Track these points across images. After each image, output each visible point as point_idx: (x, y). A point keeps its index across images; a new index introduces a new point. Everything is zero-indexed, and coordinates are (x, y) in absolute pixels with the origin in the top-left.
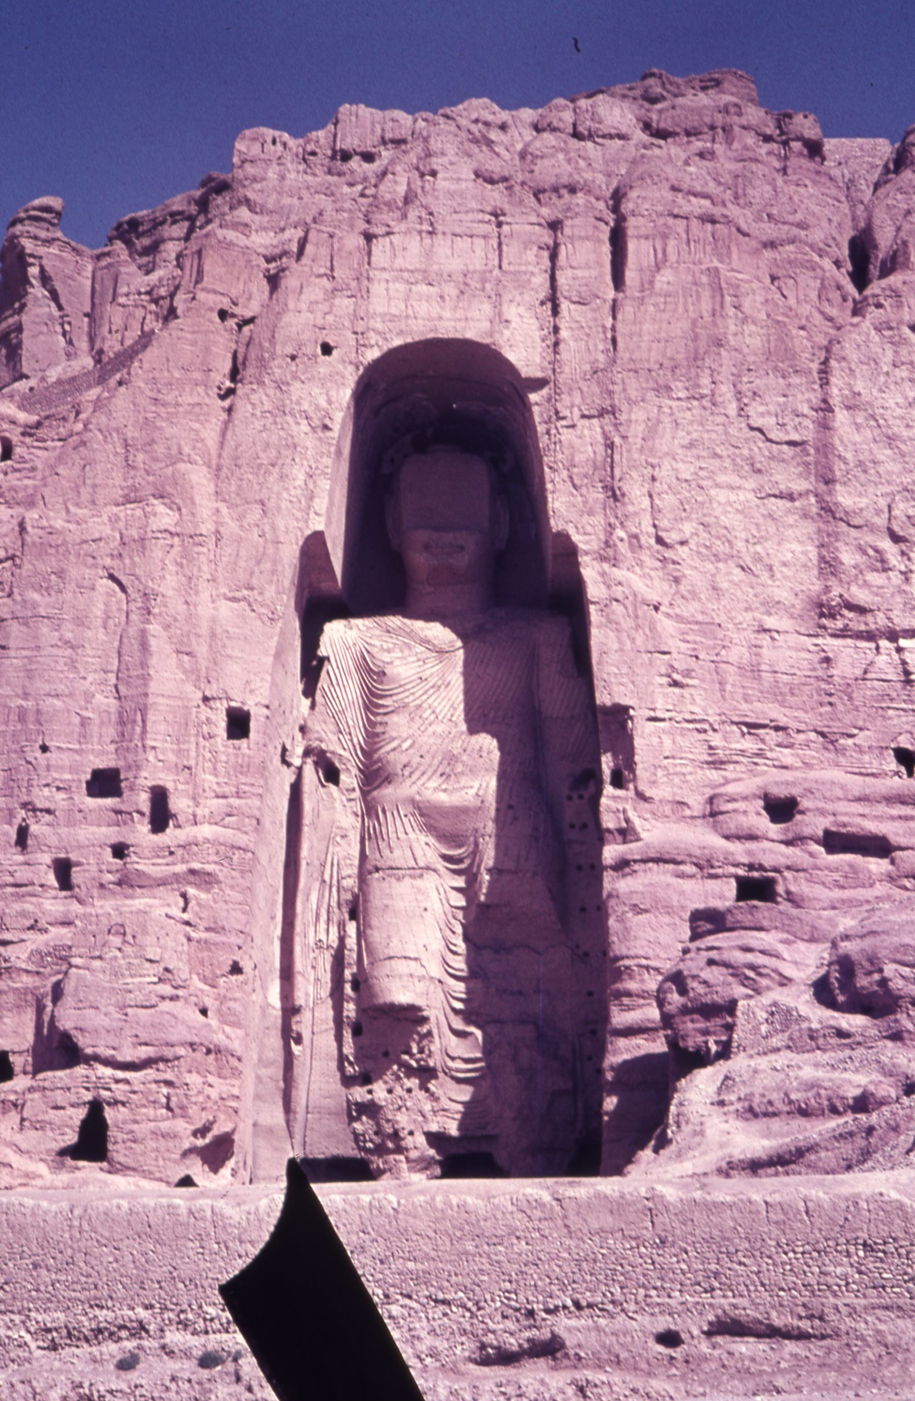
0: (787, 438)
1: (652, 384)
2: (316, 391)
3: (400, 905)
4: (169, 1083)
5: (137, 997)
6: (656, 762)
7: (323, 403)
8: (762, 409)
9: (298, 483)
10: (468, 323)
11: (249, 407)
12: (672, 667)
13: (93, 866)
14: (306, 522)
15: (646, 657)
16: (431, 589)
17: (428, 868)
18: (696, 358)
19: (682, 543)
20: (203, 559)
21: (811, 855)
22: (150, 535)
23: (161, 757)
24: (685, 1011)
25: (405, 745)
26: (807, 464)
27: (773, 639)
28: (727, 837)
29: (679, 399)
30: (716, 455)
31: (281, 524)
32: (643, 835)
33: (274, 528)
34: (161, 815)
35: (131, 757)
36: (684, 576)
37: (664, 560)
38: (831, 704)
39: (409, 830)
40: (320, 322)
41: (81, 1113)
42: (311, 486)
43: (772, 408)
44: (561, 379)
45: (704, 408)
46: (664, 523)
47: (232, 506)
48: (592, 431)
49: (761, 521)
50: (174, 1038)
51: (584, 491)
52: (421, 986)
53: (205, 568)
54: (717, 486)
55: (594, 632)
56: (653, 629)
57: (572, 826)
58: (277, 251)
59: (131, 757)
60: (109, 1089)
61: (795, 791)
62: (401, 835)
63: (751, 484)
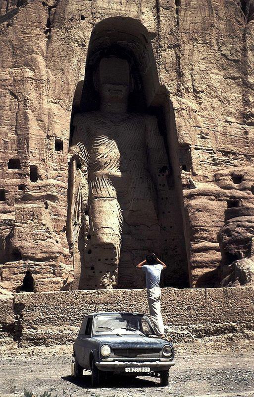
0: (233, 58)
1: (191, 38)
2: (80, 32)
3: (105, 210)
4: (53, 266)
5: (40, 236)
6: (198, 163)
7: (82, 36)
8: (225, 48)
9: (74, 64)
10: (131, 12)
11: (57, 36)
12: (202, 132)
14: (78, 77)
15: (194, 128)
16: (109, 104)
17: (114, 198)
18: (204, 30)
19: (202, 92)
20: (44, 88)
21: (248, 193)
22: (25, 79)
23: (34, 156)
24: (230, 242)
25: (105, 156)
26: (239, 68)
27: (230, 125)
28: (221, 188)
29: (200, 43)
30: (212, 63)
31: (69, 78)
32: (196, 186)
33: (67, 78)
34: (34, 175)
35: (24, 155)
36: (203, 102)
37: (196, 97)
38: (248, 146)
39: (107, 185)
40: (79, 8)
41: (23, 276)
42: (79, 65)
43: (229, 48)
44: (161, 33)
45: (208, 47)
46: (196, 85)
47: (53, 70)
49: (225, 85)
50: (55, 250)
51: (170, 72)
52: (113, 237)
53: (44, 91)
54: (212, 73)
55: (176, 119)
56: (195, 119)
57: (160, 185)
59: (24, 155)
60: (33, 268)
61: (242, 173)
62: (105, 186)
63: (222, 73)
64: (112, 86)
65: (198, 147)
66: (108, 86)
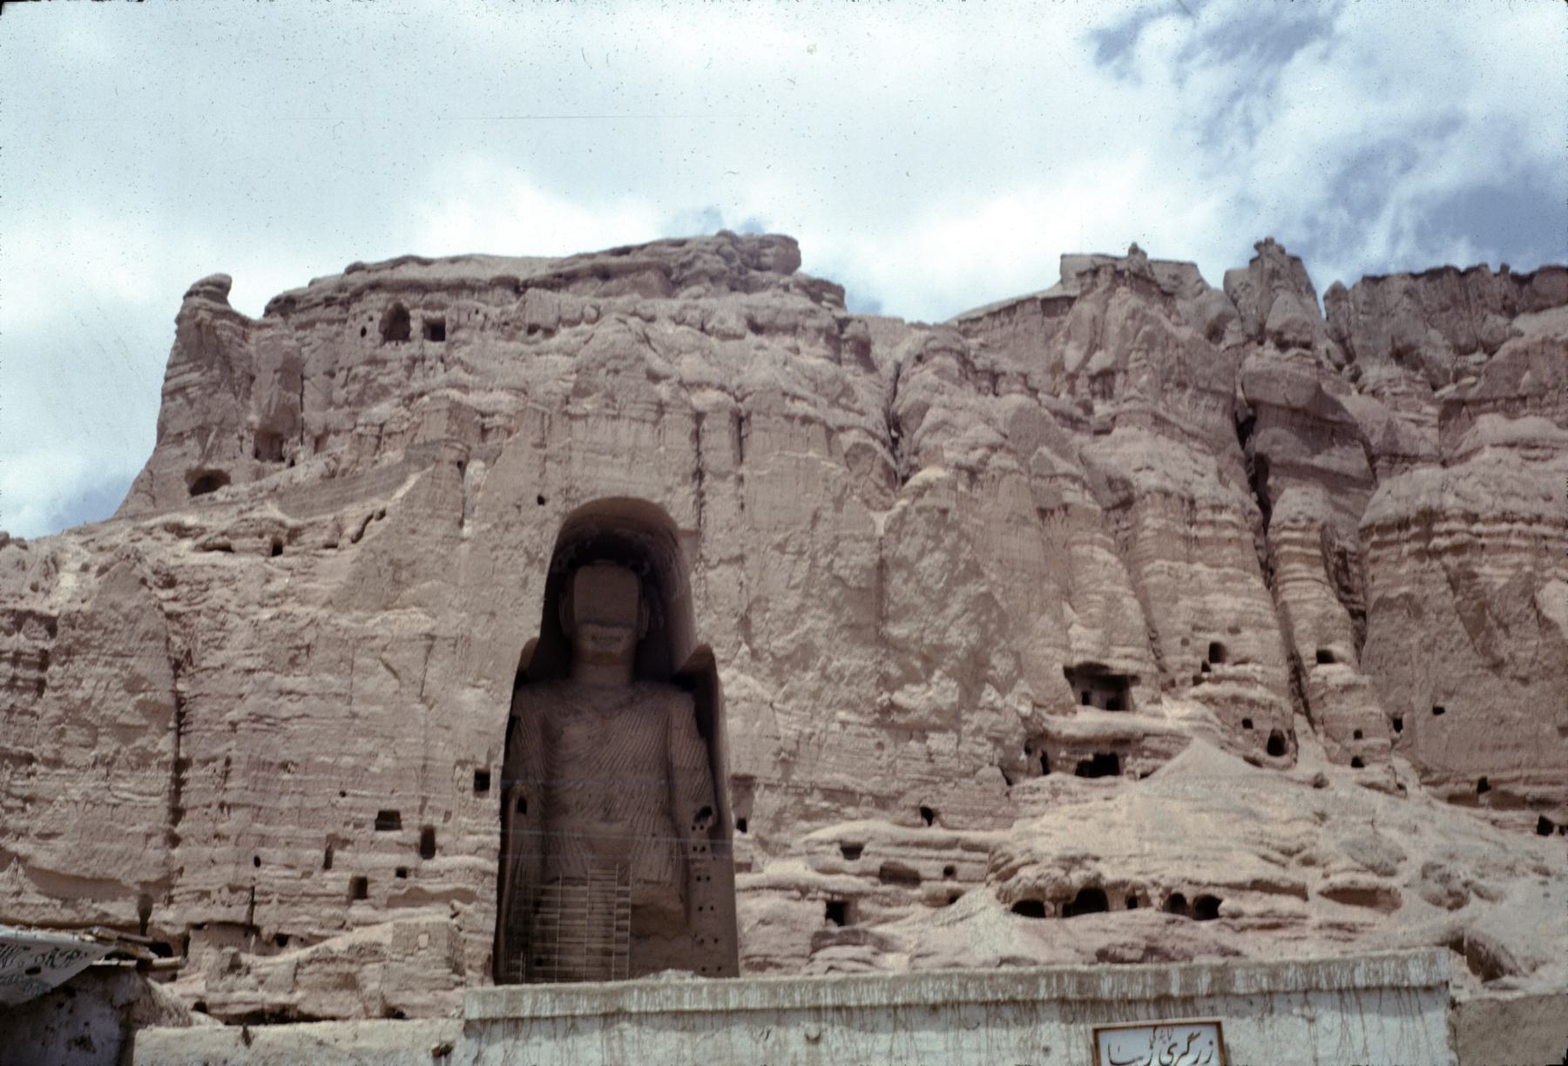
13: (383, 885)
48: (727, 572)
58: (492, 409)
63: (832, 617)
64: (600, 630)
66: (592, 629)
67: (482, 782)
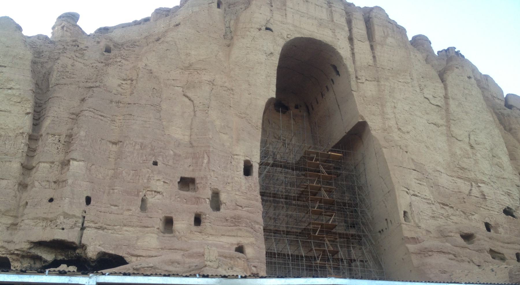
8: (428, 92)
65: (416, 193)
67: (248, 170)
